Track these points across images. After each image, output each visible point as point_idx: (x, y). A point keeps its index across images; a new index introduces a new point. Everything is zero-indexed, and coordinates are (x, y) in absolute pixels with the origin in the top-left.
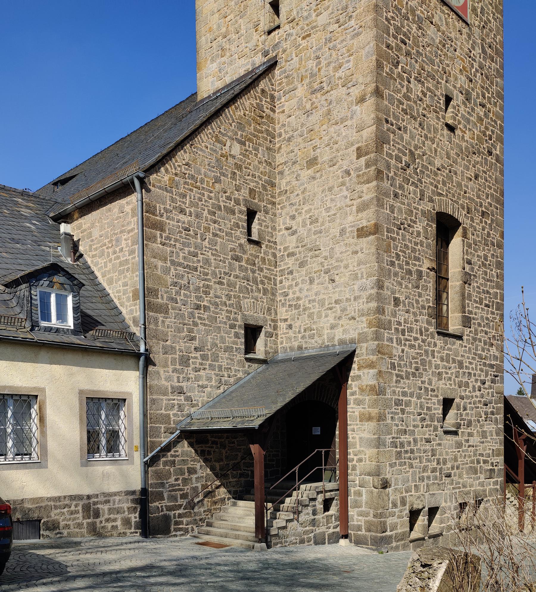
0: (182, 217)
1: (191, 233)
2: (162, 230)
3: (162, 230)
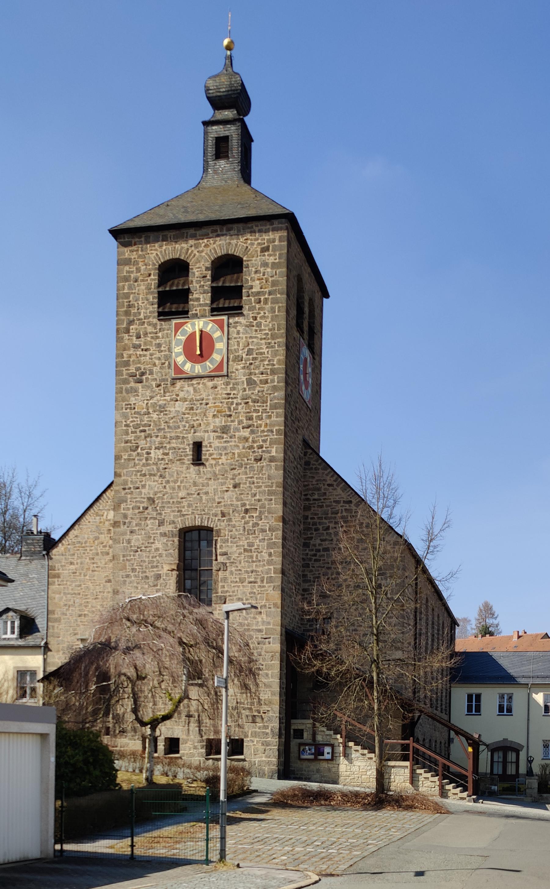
0: (72, 567)
1: (78, 574)
2: (59, 577)
3: (59, 577)
